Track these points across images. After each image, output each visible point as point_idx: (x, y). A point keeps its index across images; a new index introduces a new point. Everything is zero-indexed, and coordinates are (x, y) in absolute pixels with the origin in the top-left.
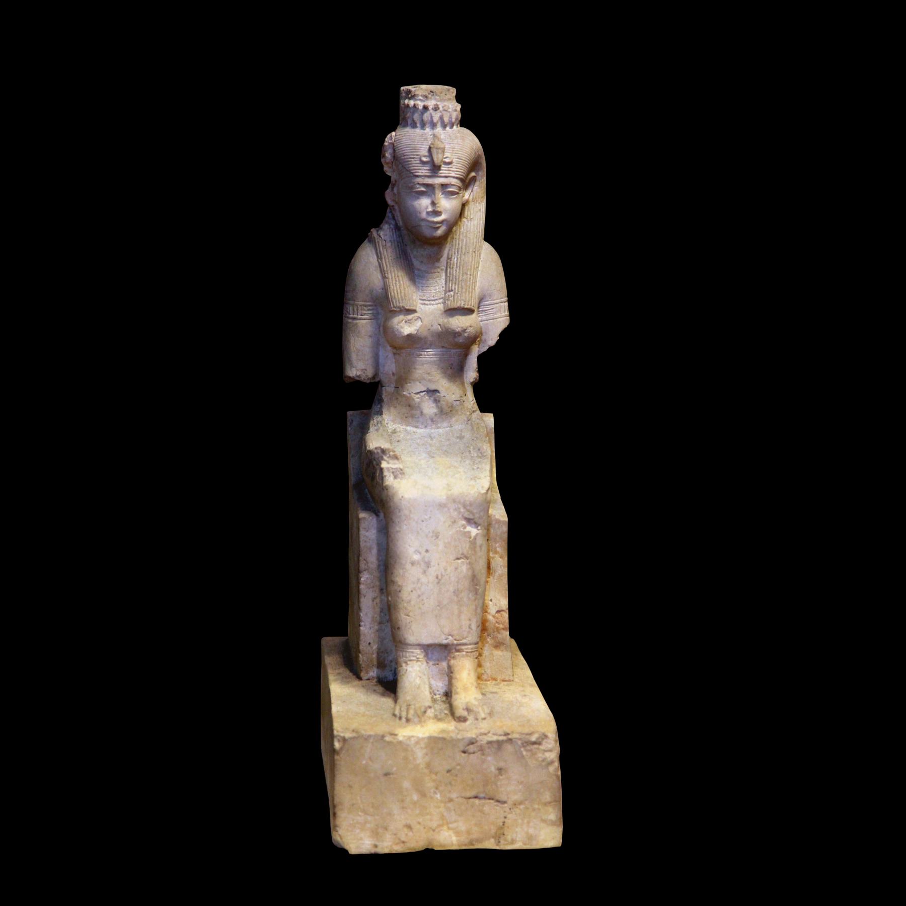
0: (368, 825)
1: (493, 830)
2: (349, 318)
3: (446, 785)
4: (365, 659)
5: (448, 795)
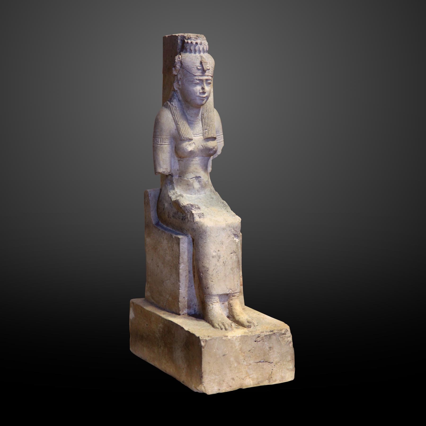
0: (216, 380)
1: (268, 376)
2: (158, 144)
3: (248, 357)
4: (182, 305)
5: (249, 362)
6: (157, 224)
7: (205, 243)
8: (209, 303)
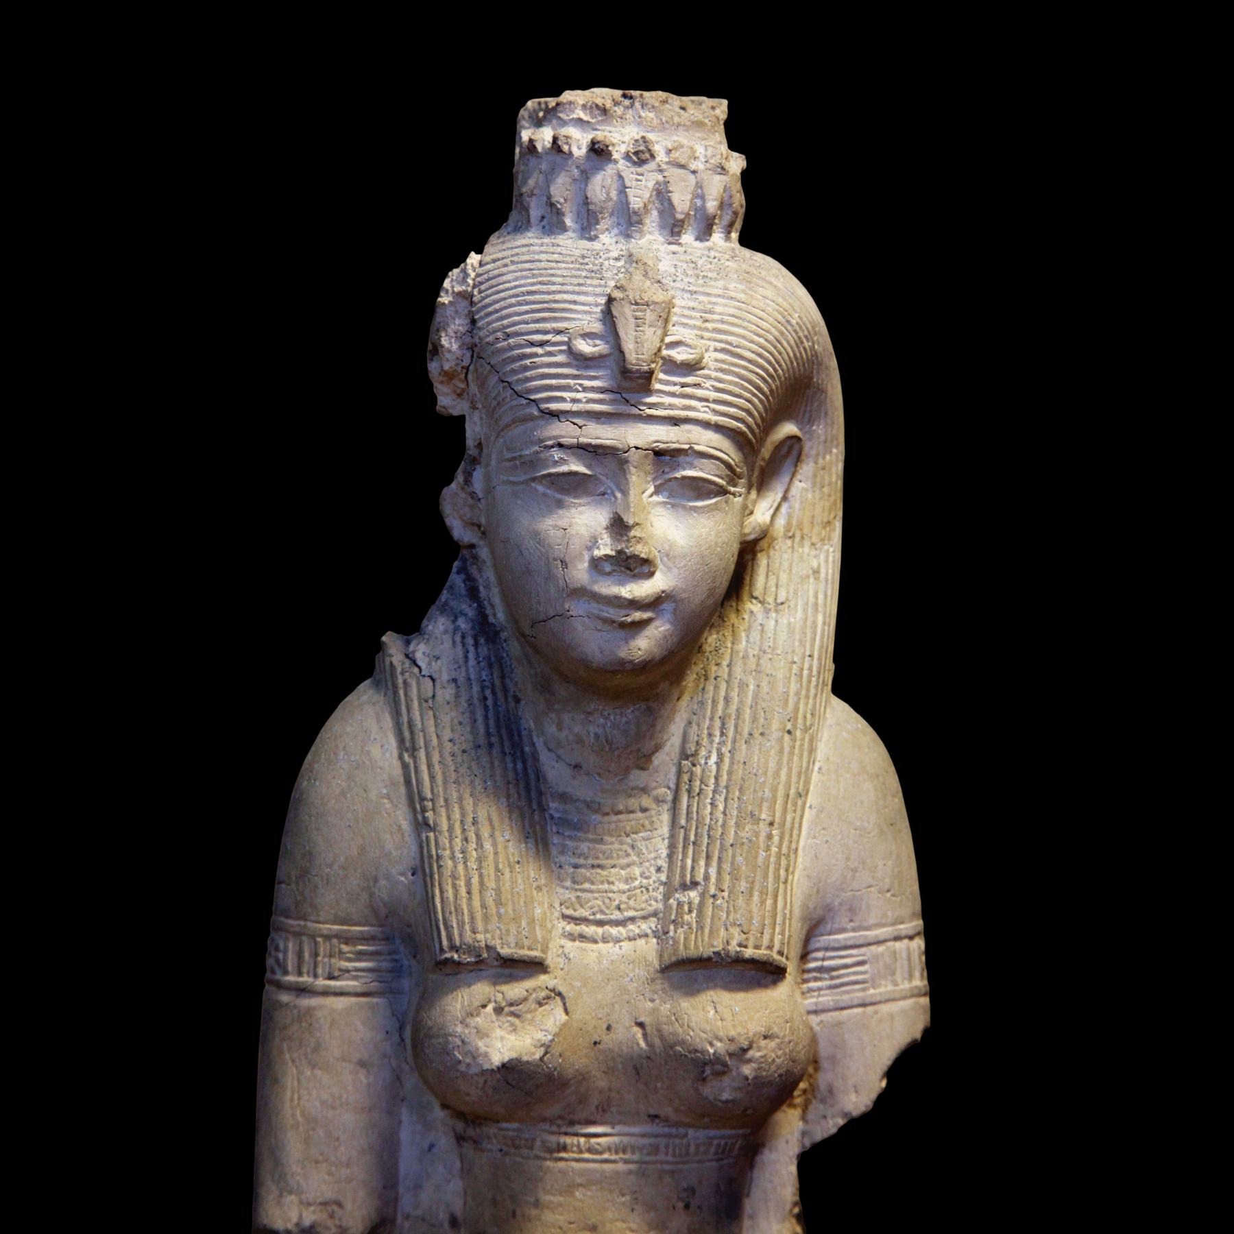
2: (280, 986)
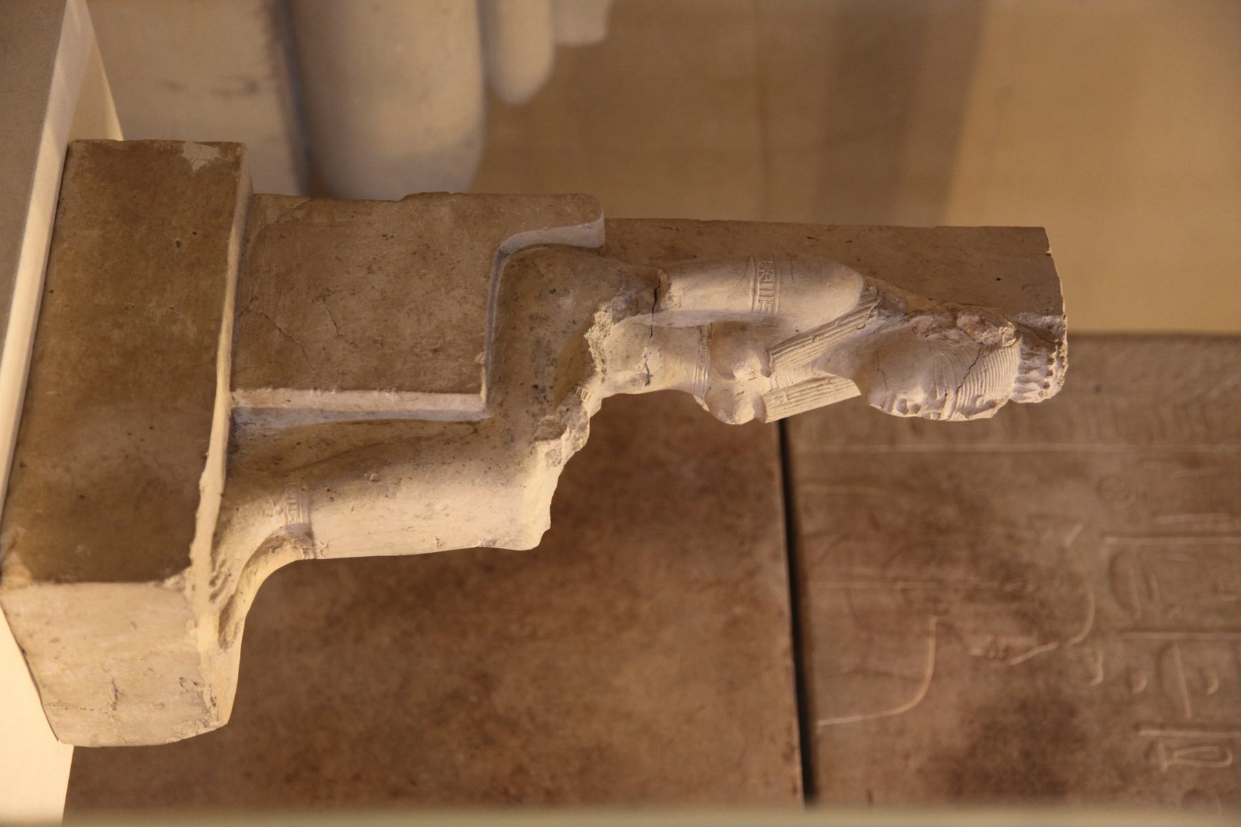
2: (756, 280)
6: (502, 255)
7: (473, 481)
8: (283, 503)
